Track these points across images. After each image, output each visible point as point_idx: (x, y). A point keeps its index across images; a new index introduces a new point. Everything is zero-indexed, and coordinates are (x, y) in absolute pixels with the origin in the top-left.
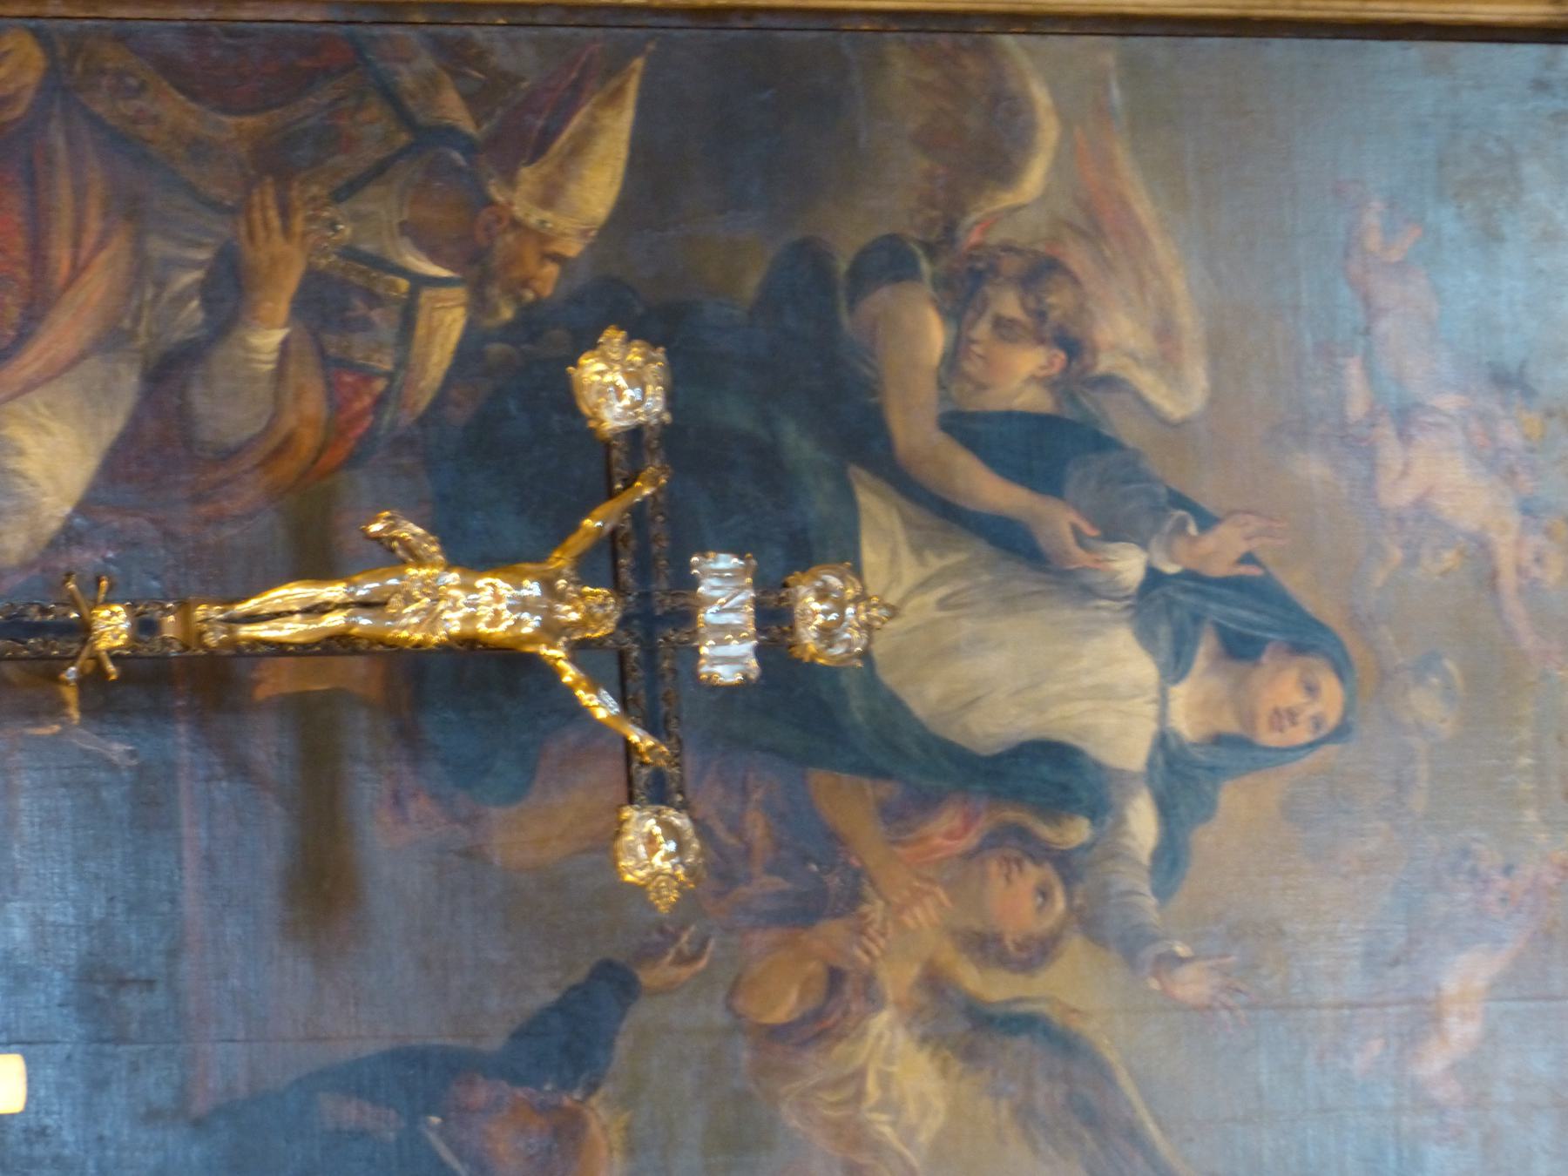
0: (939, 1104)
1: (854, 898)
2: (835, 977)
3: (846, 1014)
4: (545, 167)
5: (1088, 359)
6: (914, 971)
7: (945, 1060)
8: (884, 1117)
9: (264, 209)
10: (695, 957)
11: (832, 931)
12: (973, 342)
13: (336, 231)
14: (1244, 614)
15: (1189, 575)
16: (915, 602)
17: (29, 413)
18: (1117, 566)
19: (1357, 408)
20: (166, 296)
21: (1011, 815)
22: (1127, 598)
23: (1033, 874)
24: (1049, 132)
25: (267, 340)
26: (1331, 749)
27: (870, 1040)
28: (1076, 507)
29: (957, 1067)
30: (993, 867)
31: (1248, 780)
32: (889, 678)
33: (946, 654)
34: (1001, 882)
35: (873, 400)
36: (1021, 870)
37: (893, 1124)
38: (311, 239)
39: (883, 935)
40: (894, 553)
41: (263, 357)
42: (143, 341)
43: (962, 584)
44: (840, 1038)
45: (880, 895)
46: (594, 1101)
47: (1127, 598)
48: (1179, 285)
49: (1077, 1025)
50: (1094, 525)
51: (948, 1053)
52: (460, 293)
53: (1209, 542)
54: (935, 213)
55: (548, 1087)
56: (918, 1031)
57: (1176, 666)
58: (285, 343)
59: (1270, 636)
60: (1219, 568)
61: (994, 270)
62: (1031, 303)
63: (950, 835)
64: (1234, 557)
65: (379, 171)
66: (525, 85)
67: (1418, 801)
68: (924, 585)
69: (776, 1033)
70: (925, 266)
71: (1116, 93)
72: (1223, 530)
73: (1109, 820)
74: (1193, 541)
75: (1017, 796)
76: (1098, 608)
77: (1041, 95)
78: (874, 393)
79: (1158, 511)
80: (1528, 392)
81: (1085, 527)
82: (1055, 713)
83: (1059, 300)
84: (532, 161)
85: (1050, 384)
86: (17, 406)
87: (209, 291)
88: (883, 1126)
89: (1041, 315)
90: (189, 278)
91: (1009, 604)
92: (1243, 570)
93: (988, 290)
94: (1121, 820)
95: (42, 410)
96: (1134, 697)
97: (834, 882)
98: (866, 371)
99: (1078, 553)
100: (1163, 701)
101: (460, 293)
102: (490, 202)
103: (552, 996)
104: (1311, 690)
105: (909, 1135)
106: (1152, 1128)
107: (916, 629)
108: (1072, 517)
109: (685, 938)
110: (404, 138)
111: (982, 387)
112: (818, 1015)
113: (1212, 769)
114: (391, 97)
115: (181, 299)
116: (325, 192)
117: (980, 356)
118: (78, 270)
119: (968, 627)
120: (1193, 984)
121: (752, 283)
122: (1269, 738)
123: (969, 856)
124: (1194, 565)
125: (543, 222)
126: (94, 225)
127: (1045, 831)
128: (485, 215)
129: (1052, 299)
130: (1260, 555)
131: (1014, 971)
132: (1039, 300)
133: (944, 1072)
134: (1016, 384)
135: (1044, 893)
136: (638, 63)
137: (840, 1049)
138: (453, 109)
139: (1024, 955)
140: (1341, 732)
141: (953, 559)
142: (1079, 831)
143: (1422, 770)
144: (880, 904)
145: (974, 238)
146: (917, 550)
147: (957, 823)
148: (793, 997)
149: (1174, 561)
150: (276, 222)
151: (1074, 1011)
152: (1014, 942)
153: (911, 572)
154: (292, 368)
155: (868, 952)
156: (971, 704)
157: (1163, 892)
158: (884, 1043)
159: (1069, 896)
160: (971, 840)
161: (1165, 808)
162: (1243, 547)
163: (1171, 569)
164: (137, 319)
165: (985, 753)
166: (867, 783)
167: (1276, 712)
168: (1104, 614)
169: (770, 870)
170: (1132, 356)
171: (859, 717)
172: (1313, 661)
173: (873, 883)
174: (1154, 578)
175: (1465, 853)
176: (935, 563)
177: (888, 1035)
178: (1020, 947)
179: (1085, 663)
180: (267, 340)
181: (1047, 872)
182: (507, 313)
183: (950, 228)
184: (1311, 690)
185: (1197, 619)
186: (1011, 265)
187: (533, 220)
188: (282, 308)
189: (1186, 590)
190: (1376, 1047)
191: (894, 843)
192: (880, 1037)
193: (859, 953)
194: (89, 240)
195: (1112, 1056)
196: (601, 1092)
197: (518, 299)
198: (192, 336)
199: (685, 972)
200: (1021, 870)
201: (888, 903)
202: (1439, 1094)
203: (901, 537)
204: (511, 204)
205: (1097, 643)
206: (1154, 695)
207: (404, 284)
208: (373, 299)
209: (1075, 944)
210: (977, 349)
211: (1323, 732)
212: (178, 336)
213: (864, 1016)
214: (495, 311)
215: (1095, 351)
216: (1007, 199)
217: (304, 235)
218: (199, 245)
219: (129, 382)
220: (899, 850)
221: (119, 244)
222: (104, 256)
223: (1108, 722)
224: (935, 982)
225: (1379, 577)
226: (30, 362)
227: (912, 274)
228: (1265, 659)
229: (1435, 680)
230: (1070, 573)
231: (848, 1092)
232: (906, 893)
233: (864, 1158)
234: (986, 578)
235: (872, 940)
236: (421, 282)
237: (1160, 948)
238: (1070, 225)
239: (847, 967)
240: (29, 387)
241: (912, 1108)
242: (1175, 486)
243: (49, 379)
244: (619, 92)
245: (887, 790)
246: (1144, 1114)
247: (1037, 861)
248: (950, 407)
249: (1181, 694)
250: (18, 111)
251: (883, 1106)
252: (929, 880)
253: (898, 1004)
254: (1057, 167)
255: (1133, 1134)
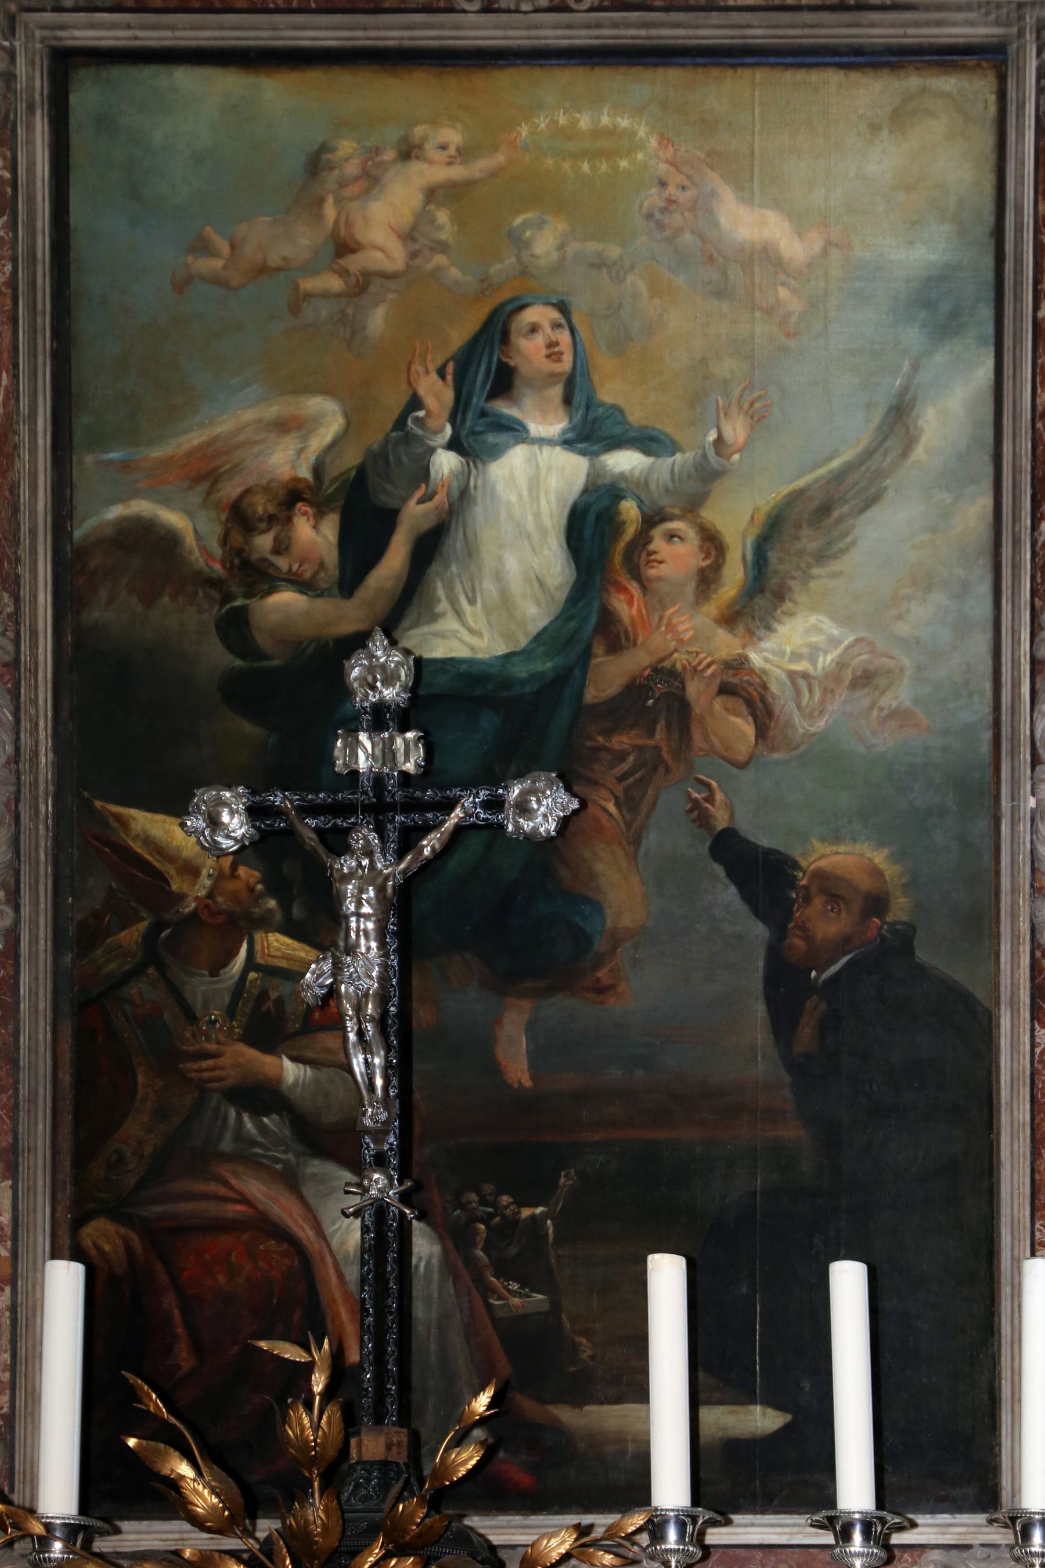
0: (813, 619)
1: (672, 674)
2: (726, 690)
3: (749, 683)
4: (170, 871)
5: (301, 486)
6: (722, 635)
7: (784, 613)
8: (821, 659)
9: (201, 1071)
10: (708, 786)
11: (693, 689)
12: (290, 570)
13: (216, 1021)
14: (480, 378)
15: (452, 419)
16: (471, 622)
17: (338, 1235)
18: (446, 471)
19: (335, 284)
20: (260, 1139)
21: (618, 558)
22: (468, 465)
23: (658, 543)
24: (142, 507)
25: (291, 1071)
26: (575, 319)
27: (768, 666)
28: (405, 500)
29: (788, 605)
30: (652, 572)
31: (596, 379)
32: (523, 642)
33: (506, 599)
34: (662, 566)
35: (331, 644)
36: (655, 552)
37: (826, 653)
38: (222, 1038)
39: (698, 654)
40: (438, 635)
41: (302, 1073)
42: (290, 1156)
43: (459, 588)
44: (765, 686)
45: (671, 654)
46: (804, 864)
47: (468, 465)
48: (248, 415)
49: (761, 517)
50: (418, 488)
51: (779, 612)
52: (258, 936)
53: (430, 401)
54: (201, 593)
55: (794, 895)
56: (762, 632)
57: (515, 431)
58: (293, 1059)
59: (495, 359)
60: (449, 395)
61: (239, 552)
62: (263, 526)
63: (630, 603)
64: (441, 382)
65: (176, 992)
66: (114, 885)
67: (614, 252)
68: (459, 614)
69: (762, 732)
70: (238, 603)
71: (112, 455)
72: (421, 391)
73: (623, 485)
74: (429, 414)
75: (604, 555)
76: (475, 487)
77: (115, 512)
78: (327, 644)
79: (408, 439)
80: (324, 148)
81: (419, 493)
82: (547, 521)
83: (261, 506)
84: (169, 884)
85: (319, 515)
86: (335, 1243)
87: (258, 1110)
88: (826, 660)
89: (271, 519)
90: (249, 1125)
91: (471, 552)
92: (449, 378)
93: (254, 557)
94: (622, 476)
95: (337, 1226)
96: (537, 464)
97: (661, 688)
98: (311, 649)
99: (437, 498)
100: (541, 441)
101: (258, 936)
102: (195, 913)
103: (733, 890)
104: (534, 329)
105: (834, 642)
106: (835, 464)
107: (488, 622)
108: (412, 502)
109: (696, 795)
110: (151, 971)
111: (322, 565)
112: (750, 703)
113: (588, 407)
114: (126, 979)
115: (262, 1129)
116: (189, 1028)
117: (300, 566)
118: (245, 1200)
119: (489, 585)
120: (736, 430)
121: (249, 728)
122: (566, 364)
123: (644, 588)
124: (446, 414)
125: (209, 876)
126: (213, 1187)
127: (630, 532)
128: (205, 916)
129: (260, 510)
130: (439, 363)
131: (724, 561)
132: (261, 520)
133: (791, 614)
134: (319, 539)
135: (671, 536)
136: (98, 804)
137: (774, 688)
138: (132, 935)
139: (713, 553)
140: (563, 308)
141: (441, 592)
142: (630, 510)
143: (592, 246)
144: (676, 655)
145: (218, 567)
146: (435, 617)
147: (622, 597)
148: (738, 721)
149: (441, 430)
150: (210, 1063)
151: (752, 518)
152: (704, 559)
153: (450, 623)
154: (309, 1054)
155: (709, 666)
156: (541, 584)
157: (673, 448)
158: (771, 657)
159: (671, 518)
160: (634, 587)
161: (616, 443)
162: (434, 376)
163: (448, 430)
164: (277, 1160)
165: (575, 575)
166: (594, 661)
167: (548, 356)
168: (480, 482)
169: (651, 734)
170: (300, 452)
171: (549, 665)
172: (514, 327)
173: (662, 660)
174: (454, 445)
175: (650, 216)
176: (443, 606)
177: (766, 654)
178: (707, 555)
179: (513, 498)
180: (291, 1071)
181: (657, 533)
182: (272, 903)
183: (212, 583)
184: (534, 329)
185: (483, 414)
186: (237, 538)
187: (208, 883)
188: (268, 1059)
189: (464, 420)
190: (783, 293)
191: (635, 644)
192: (766, 660)
193: (709, 672)
194: (223, 1191)
195: (785, 490)
196: (799, 859)
197: (261, 895)
198: (288, 1123)
199: (719, 796)
200: (655, 552)
201: (676, 650)
202: (817, 247)
203: (425, 629)
204: (197, 898)
205: (500, 488)
206: (536, 448)
207: (252, 975)
208: (263, 995)
209: (708, 514)
210: (295, 568)
211: (563, 321)
212: (287, 1132)
213: (751, 671)
214: (270, 911)
215: (297, 480)
216: (190, 540)
217: (219, 1043)
218: (226, 1118)
219: (317, 1167)
220: (640, 640)
221: (224, 1170)
222: (233, 1182)
223: (553, 482)
224: (730, 619)
225: (454, 273)
226: (305, 1233)
227: (243, 610)
228: (512, 363)
229: (528, 234)
230: (451, 505)
231: (802, 683)
232: (669, 636)
233: (848, 675)
234: (454, 568)
235: (700, 663)
236: (250, 964)
237: (711, 452)
238: (209, 493)
239: (718, 681)
240: (321, 1234)
241: (815, 639)
242: (390, 425)
243: (315, 1217)
244: (118, 817)
245: (599, 649)
246: (823, 471)
247: (649, 540)
248: (336, 591)
249: (535, 429)
250: (134, 1236)
251: (813, 660)
252: (661, 619)
253: (744, 646)
254: (166, 502)
255: (840, 476)
